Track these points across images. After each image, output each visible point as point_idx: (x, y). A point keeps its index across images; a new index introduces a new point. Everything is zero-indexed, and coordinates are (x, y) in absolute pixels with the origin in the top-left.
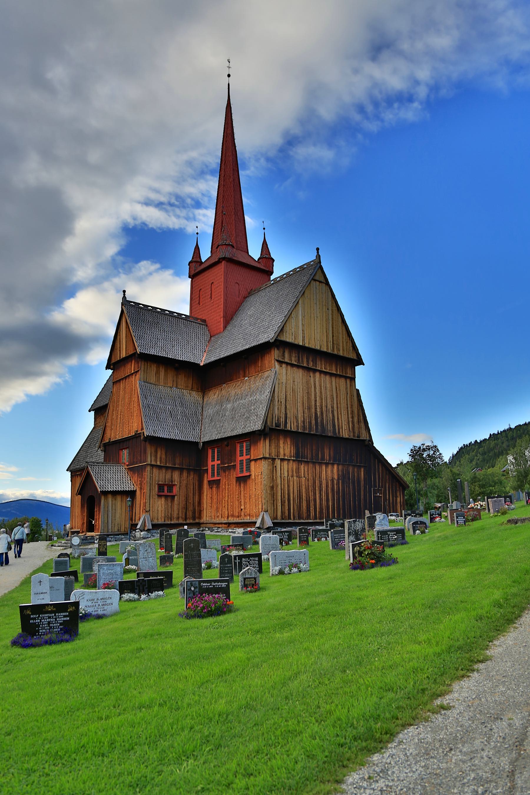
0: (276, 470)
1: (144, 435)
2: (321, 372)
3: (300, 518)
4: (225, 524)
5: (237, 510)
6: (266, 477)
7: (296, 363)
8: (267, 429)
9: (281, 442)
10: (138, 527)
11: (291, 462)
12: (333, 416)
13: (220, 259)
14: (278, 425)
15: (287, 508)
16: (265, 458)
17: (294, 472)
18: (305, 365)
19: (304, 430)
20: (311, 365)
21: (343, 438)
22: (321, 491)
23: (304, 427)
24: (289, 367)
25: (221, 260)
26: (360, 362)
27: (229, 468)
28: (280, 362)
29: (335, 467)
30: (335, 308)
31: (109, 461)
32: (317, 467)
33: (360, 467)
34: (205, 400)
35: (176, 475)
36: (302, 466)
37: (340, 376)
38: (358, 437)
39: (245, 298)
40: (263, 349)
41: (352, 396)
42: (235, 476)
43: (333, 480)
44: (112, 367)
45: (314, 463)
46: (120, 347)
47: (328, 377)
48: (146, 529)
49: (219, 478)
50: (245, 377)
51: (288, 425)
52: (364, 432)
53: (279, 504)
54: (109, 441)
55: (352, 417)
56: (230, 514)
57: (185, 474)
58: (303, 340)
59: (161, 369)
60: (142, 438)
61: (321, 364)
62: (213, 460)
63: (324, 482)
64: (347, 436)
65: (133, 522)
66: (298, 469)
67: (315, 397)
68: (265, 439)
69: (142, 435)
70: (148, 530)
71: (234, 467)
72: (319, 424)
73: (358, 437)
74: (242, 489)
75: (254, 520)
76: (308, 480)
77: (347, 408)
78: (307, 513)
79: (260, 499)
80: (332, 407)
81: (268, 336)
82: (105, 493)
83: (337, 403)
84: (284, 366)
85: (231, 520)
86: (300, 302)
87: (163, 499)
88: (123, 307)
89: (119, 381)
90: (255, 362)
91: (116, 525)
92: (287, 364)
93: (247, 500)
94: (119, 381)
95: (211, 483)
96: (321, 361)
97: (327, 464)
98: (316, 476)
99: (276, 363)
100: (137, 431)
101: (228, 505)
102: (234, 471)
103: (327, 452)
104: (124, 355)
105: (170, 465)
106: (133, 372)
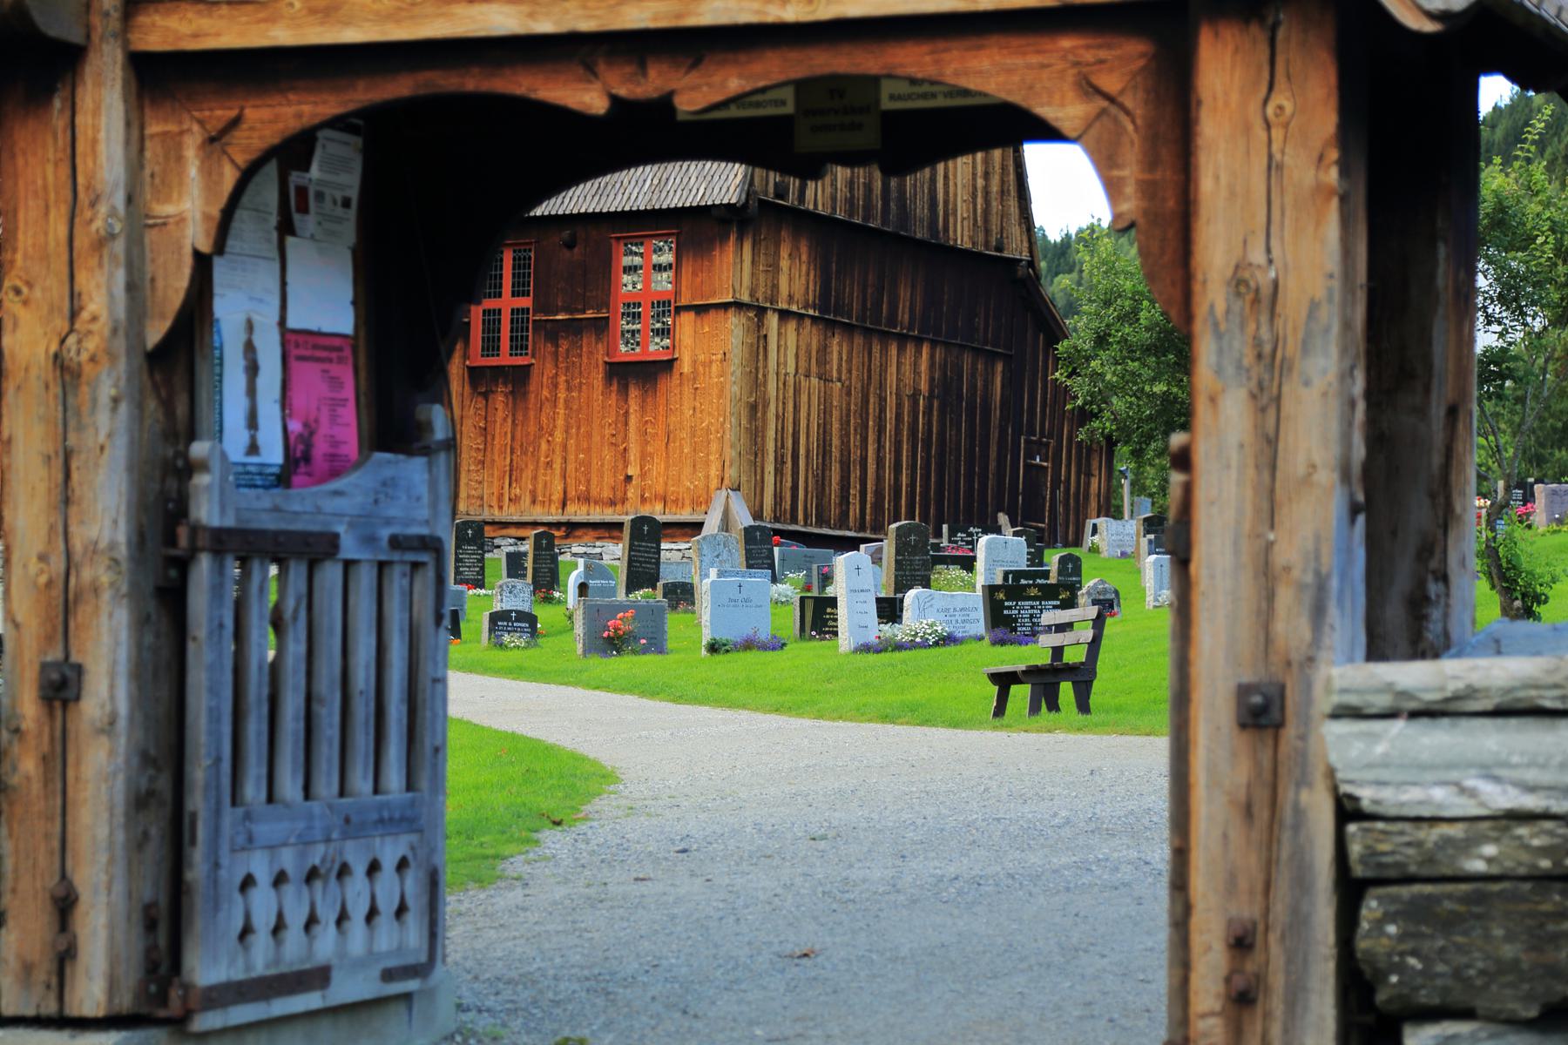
3: (820, 523)
5: (608, 479)
6: (738, 373)
8: (753, 204)
9: (784, 253)
11: (808, 322)
15: (789, 484)
16: (738, 305)
17: (814, 361)
19: (851, 215)
23: (851, 201)
27: (574, 329)
29: (925, 350)
32: (876, 349)
33: (992, 357)
36: (836, 340)
38: (999, 248)
42: (601, 357)
45: (868, 332)
49: (520, 361)
53: (770, 468)
55: (987, 176)
56: (572, 493)
63: (891, 401)
64: (968, 245)
66: (824, 350)
68: (740, 240)
71: (600, 327)
75: (685, 516)
76: (849, 394)
78: (841, 504)
79: (714, 447)
85: (577, 513)
93: (656, 446)
95: (479, 378)
97: (902, 339)
98: (869, 377)
101: (565, 460)
102: (598, 339)
103: (904, 294)
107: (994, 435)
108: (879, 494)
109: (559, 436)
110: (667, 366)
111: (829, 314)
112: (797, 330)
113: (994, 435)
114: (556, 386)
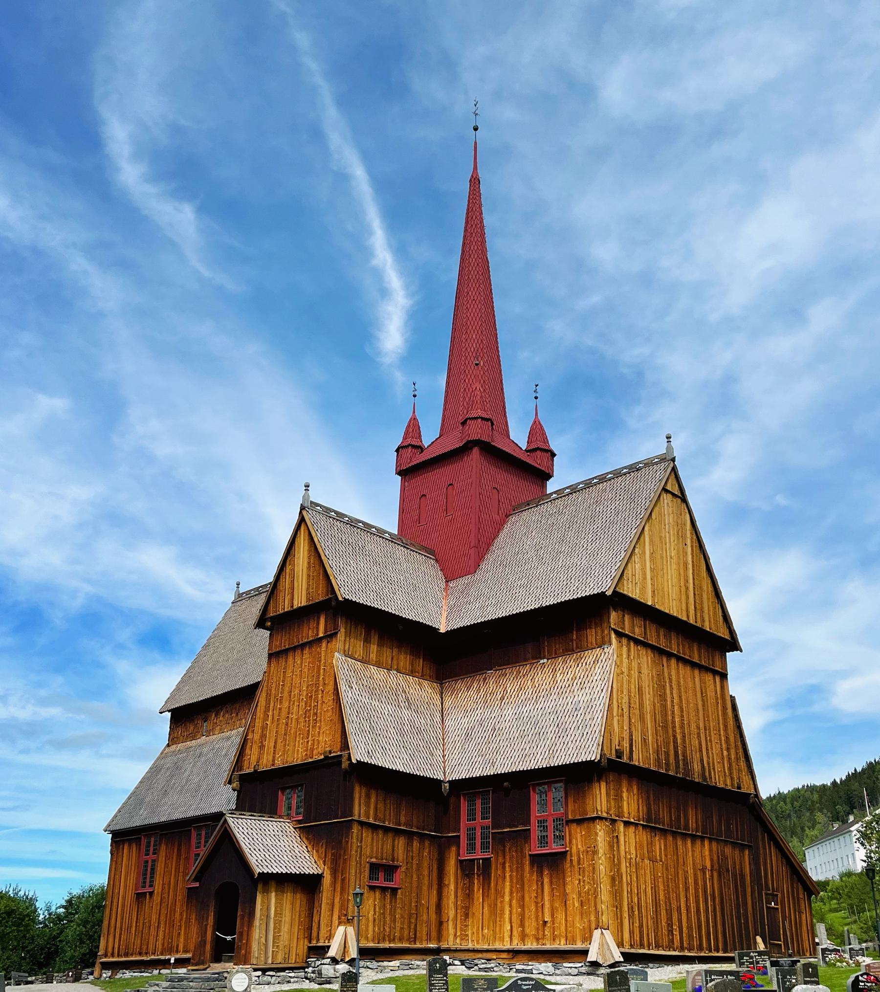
0: (618, 842)
1: (350, 758)
2: (679, 659)
3: (657, 947)
4: (508, 951)
8: (604, 762)
10: (332, 953)
11: (641, 828)
12: (700, 744)
14: (619, 754)
20: (662, 644)
21: (715, 788)
22: (687, 890)
23: (658, 760)
24: (632, 644)
26: (733, 645)
29: (706, 843)
30: (696, 544)
33: (742, 847)
35: (401, 842)
36: (657, 838)
38: (739, 788)
39: (507, 516)
41: (724, 708)
43: (703, 870)
48: (347, 959)
50: (538, 656)
51: (635, 756)
52: (746, 778)
54: (255, 771)
55: (728, 749)
57: (416, 844)
59: (372, 634)
60: (345, 765)
62: (472, 816)
66: (651, 844)
67: (673, 706)
68: (599, 781)
69: (344, 759)
70: (352, 962)
72: (681, 757)
74: (546, 880)
75: (579, 946)
80: (698, 728)
84: (624, 641)
86: (646, 528)
87: (378, 893)
88: (304, 513)
91: (281, 947)
92: (629, 638)
95: (466, 868)
97: (694, 837)
99: (613, 636)
100: (330, 752)
102: (526, 842)
103: (691, 813)
104: (300, 600)
105: (391, 826)
106: (321, 635)
107: (749, 890)
108: (690, 928)
109: (507, 898)
110: (564, 854)
111: (651, 825)
112: (635, 832)
113: (749, 890)
114: (504, 868)
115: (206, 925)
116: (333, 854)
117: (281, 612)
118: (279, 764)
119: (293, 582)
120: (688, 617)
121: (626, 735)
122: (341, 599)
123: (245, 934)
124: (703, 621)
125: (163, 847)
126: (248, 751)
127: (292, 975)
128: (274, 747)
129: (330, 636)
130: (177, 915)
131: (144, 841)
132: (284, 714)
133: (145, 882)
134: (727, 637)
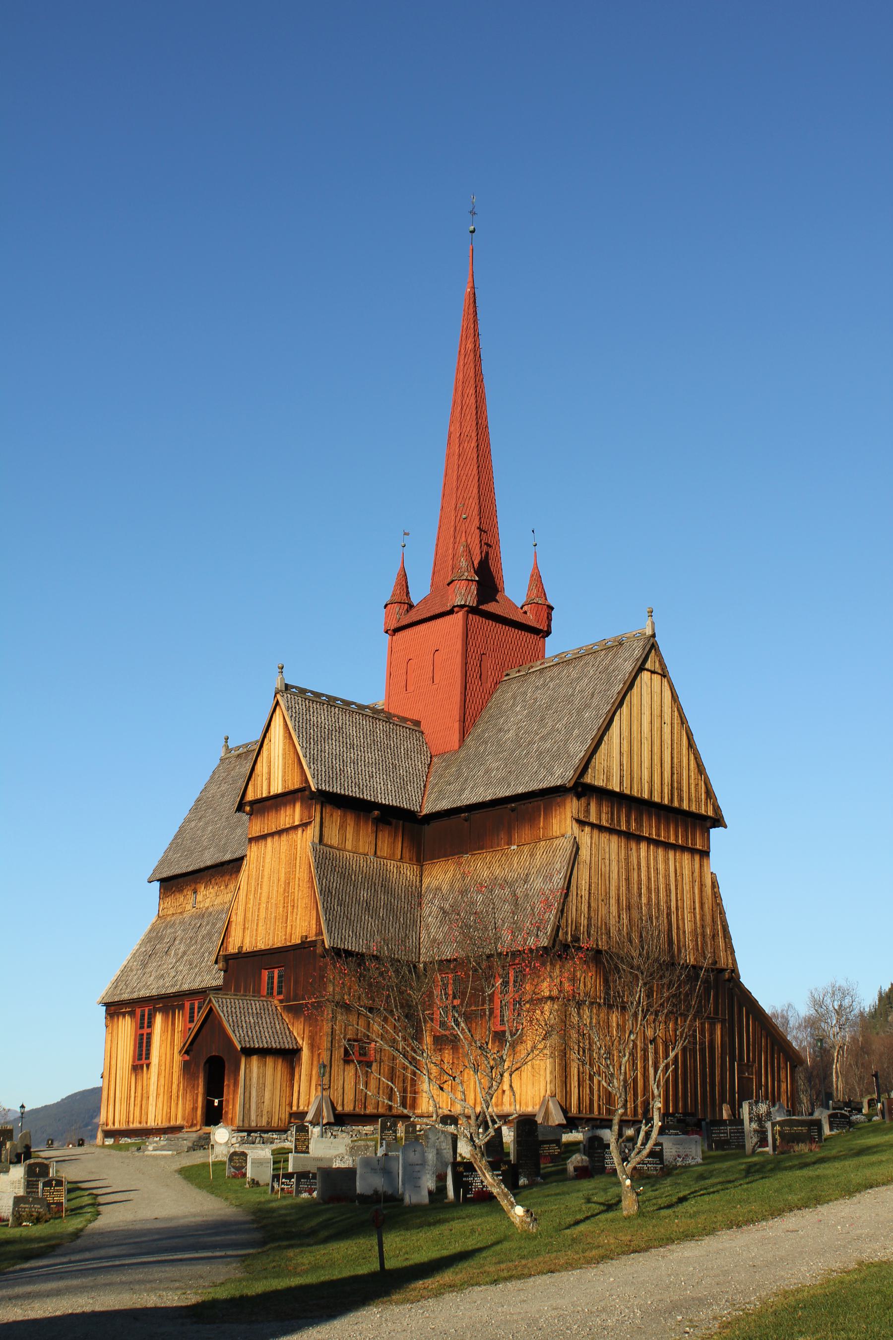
7: (608, 825)
10: (309, 1117)
13: (454, 607)
18: (624, 828)
24: (596, 832)
25: (456, 609)
26: (718, 821)
28: (581, 823)
30: (677, 721)
31: (237, 990)
34: (426, 881)
37: (683, 849)
40: (550, 796)
44: (248, 808)
46: (269, 773)
47: (660, 851)
50: (510, 843)
53: (574, 1083)
54: (239, 953)
58: (621, 783)
59: (348, 821)
60: (319, 950)
61: (651, 827)
65: (295, 1108)
67: (640, 889)
69: (319, 943)
73: (715, 963)
77: (694, 909)
80: (669, 908)
81: (561, 774)
82: (249, 1052)
83: (677, 901)
84: (587, 829)
89: (264, 837)
90: (531, 819)
91: (265, 1113)
92: (593, 826)
94: (264, 837)
95: (440, 1042)
96: (650, 819)
100: (306, 937)
104: (277, 788)
106: (297, 823)
107: (718, 1062)
113: (718, 1062)
115: (197, 1094)
116: (310, 1031)
117: (259, 796)
118: (261, 946)
119: (269, 767)
120: (662, 798)
121: (584, 921)
122: (313, 789)
123: (231, 1102)
124: (681, 800)
125: (159, 1019)
126: (233, 933)
127: (275, 1136)
128: (257, 930)
129: (304, 825)
130: (175, 1086)
131: (138, 1011)
132: (264, 899)
133: (141, 1055)
134: (710, 813)
